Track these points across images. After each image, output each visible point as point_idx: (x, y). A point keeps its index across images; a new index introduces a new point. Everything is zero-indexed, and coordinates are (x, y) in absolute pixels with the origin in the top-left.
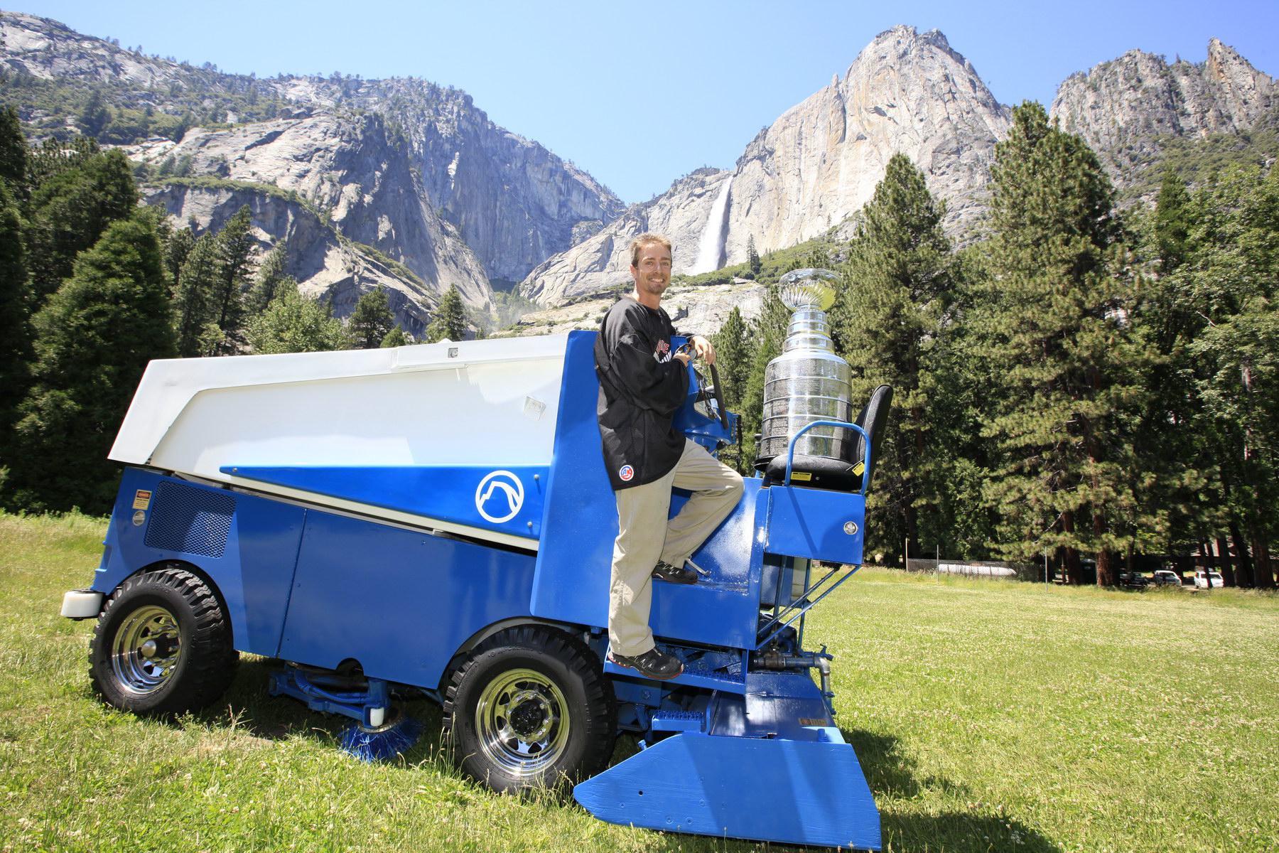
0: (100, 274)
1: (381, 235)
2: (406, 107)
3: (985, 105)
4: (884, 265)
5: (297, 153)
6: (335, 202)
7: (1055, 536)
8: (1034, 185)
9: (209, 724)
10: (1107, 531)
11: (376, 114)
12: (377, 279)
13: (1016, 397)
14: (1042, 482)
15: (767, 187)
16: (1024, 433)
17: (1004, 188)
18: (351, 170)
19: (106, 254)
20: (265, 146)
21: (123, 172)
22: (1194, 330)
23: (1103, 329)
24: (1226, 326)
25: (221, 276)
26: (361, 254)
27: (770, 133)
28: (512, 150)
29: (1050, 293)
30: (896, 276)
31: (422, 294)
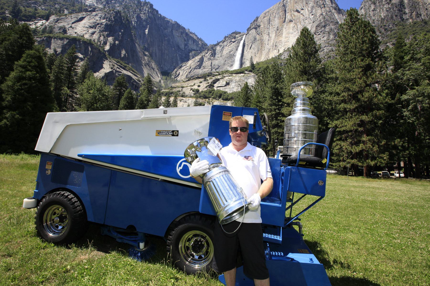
0: (23, 70)
1: (122, 56)
2: (129, 8)
3: (335, 9)
4: (298, 68)
5: (91, 25)
6: (105, 43)
7: (351, 160)
8: (352, 40)
9: (81, 247)
10: (368, 159)
11: (118, 11)
12: (121, 71)
13: (341, 114)
14: (348, 143)
15: (258, 39)
16: (343, 126)
17: (342, 41)
18: (110, 32)
19: (25, 63)
20: (79, 22)
21: (28, 32)
22: (403, 91)
23: (372, 91)
24: (414, 90)
25: (67, 70)
26: (115, 62)
27: (259, 19)
29: (356, 78)
30: (302, 72)
31: (137, 77)
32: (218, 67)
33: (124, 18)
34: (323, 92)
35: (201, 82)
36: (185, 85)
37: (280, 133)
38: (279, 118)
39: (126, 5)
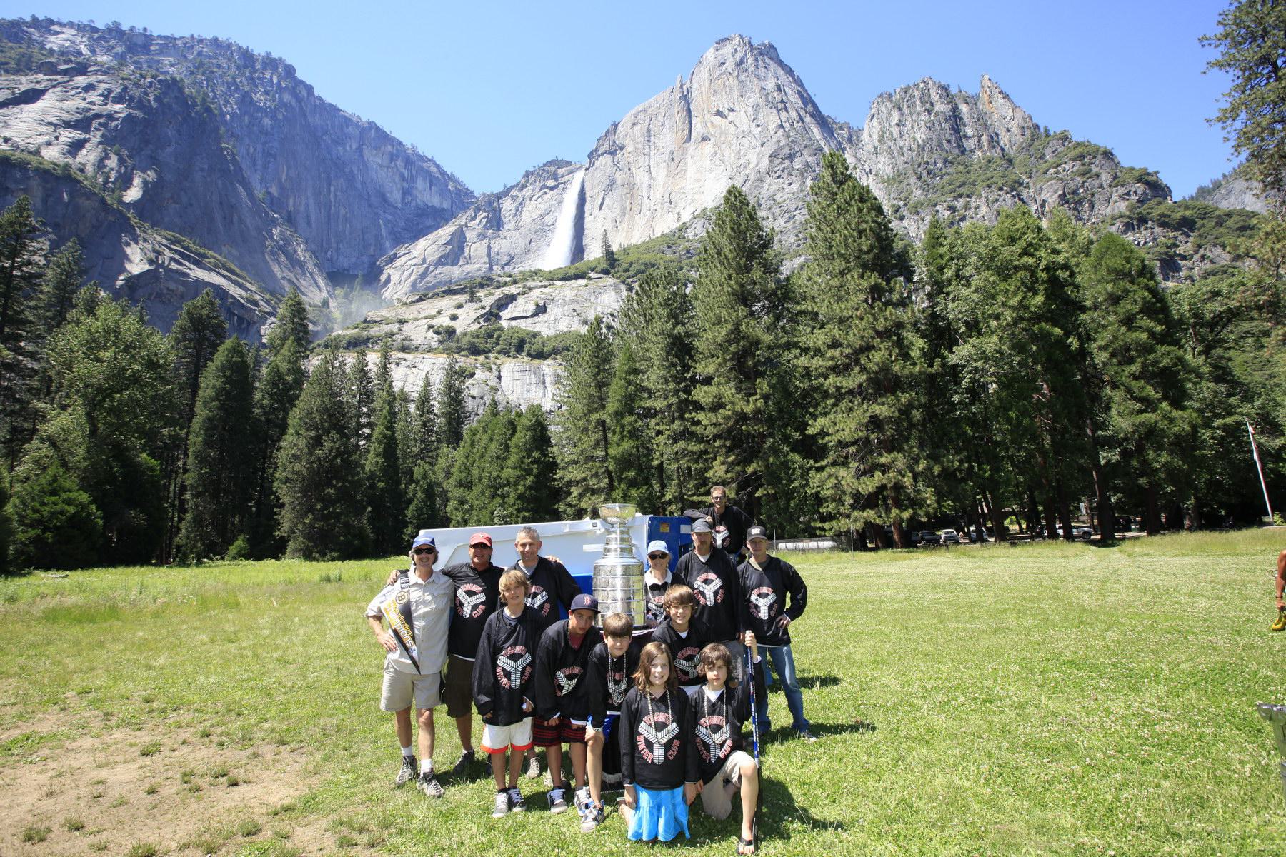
4: (725, 287)
6: (126, 182)
11: (174, 79)
12: (188, 271)
14: (853, 471)
20: (22, 106)
26: (164, 241)
28: (346, 130)
31: (247, 290)
32: (509, 258)
33: (195, 104)
34: (788, 346)
35: (459, 306)
36: (408, 313)
37: (692, 452)
38: (687, 415)
39: (201, 64)
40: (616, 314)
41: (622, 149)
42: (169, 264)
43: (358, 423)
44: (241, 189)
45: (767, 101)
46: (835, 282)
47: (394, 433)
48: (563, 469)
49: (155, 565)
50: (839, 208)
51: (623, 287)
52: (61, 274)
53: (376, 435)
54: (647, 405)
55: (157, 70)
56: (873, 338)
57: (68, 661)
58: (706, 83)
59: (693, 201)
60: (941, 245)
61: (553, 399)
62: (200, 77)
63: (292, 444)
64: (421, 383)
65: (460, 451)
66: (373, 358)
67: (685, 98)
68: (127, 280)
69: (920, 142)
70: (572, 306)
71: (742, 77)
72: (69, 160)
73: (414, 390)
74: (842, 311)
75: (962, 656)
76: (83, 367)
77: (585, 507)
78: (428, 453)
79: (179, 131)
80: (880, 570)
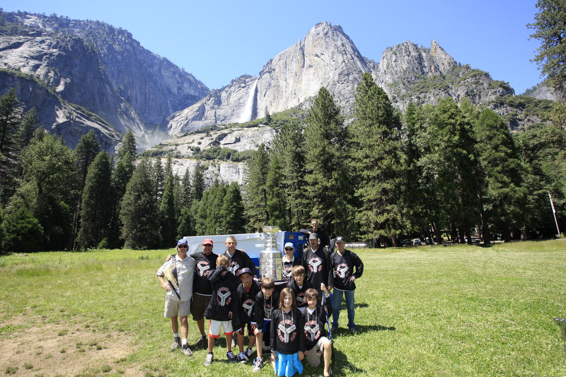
2: (96, 36)
5: (32, 54)
6: (57, 83)
11: (79, 39)
12: (84, 122)
14: (374, 212)
20: (13, 49)
26: (73, 109)
31: (109, 130)
32: (224, 118)
33: (88, 49)
35: (202, 138)
36: (179, 141)
37: (304, 204)
38: (302, 187)
39: (91, 32)
40: (271, 142)
41: (274, 70)
42: (75, 119)
43: (157, 189)
44: (107, 86)
45: (338, 50)
46: (367, 129)
47: (172, 194)
48: (247, 210)
49: (66, 251)
50: (369, 97)
51: (274, 131)
52: (28, 123)
53: (165, 194)
54: (284, 183)
55: (72, 34)
56: (384, 154)
57: (27, 293)
58: (311, 43)
59: (305, 93)
60: (414, 114)
61: (243, 180)
62: (91, 38)
63: (128, 198)
64: (185, 172)
65: (202, 202)
66: (164, 161)
67: (302, 49)
68: (57, 125)
69: (405, 69)
70: (251, 139)
71: (327, 40)
72: (33, 73)
73: (182, 175)
74: (370, 142)
75: (422, 295)
76: (37, 163)
77: (256, 227)
78: (187, 203)
79: (81, 61)
80: (386, 256)
